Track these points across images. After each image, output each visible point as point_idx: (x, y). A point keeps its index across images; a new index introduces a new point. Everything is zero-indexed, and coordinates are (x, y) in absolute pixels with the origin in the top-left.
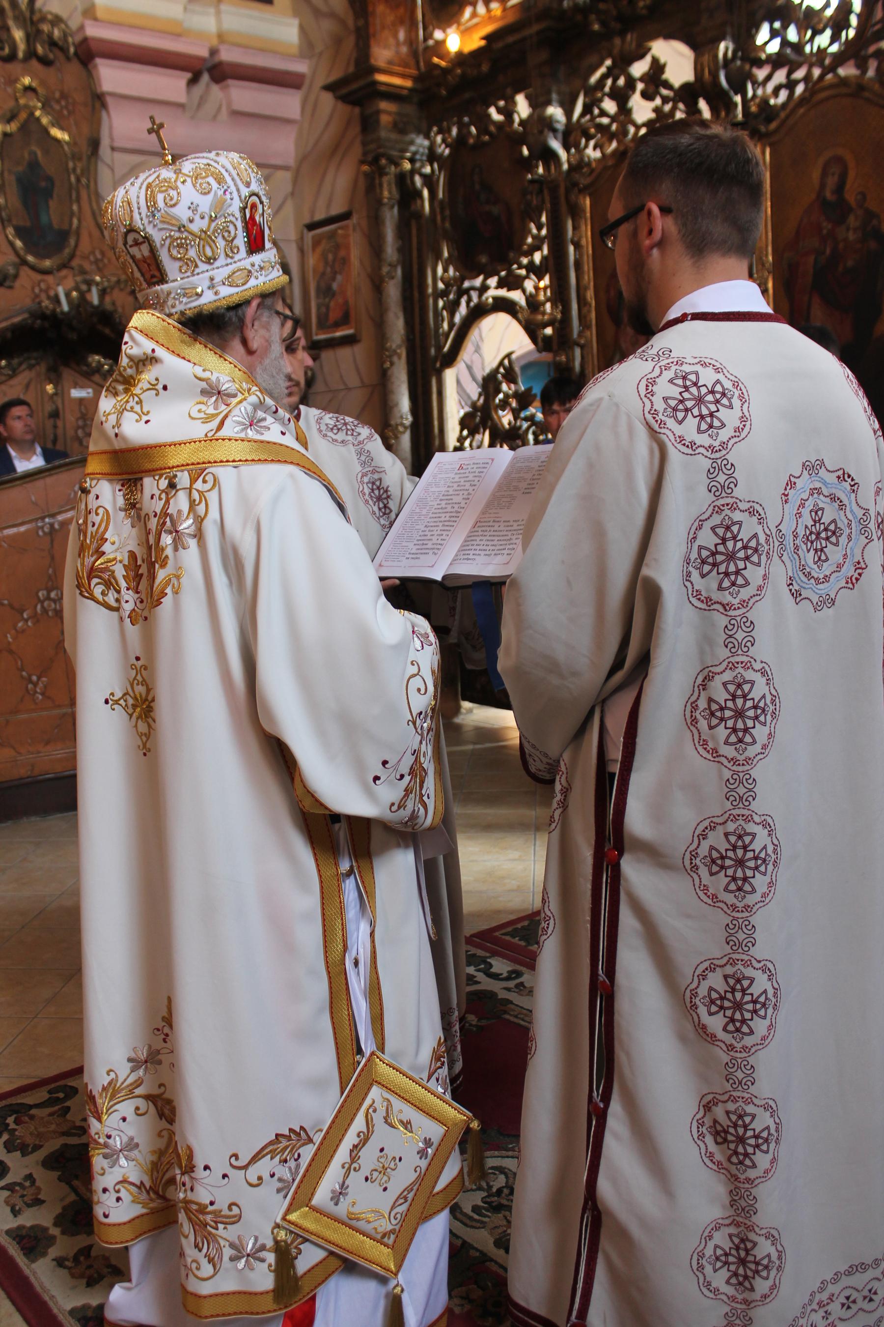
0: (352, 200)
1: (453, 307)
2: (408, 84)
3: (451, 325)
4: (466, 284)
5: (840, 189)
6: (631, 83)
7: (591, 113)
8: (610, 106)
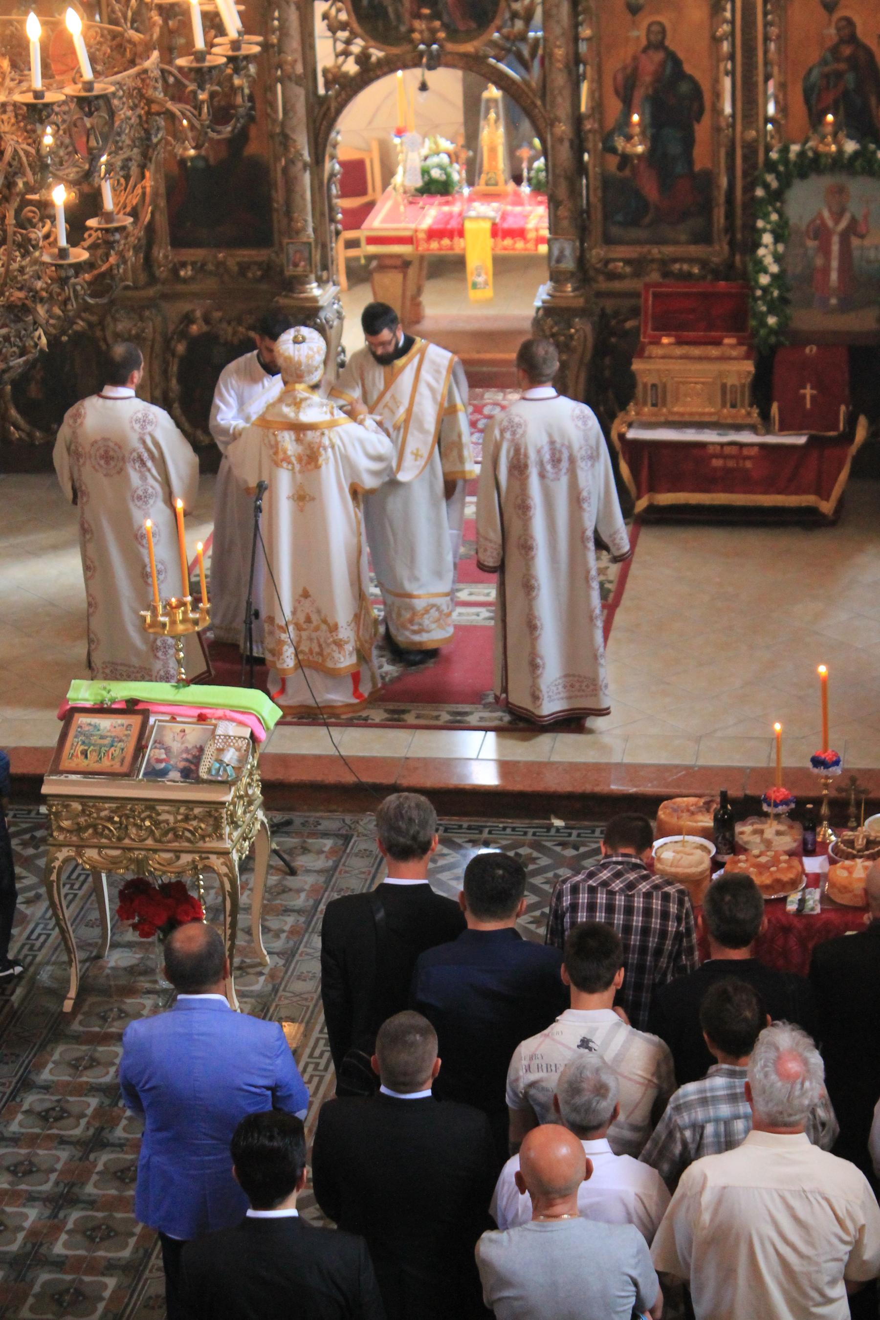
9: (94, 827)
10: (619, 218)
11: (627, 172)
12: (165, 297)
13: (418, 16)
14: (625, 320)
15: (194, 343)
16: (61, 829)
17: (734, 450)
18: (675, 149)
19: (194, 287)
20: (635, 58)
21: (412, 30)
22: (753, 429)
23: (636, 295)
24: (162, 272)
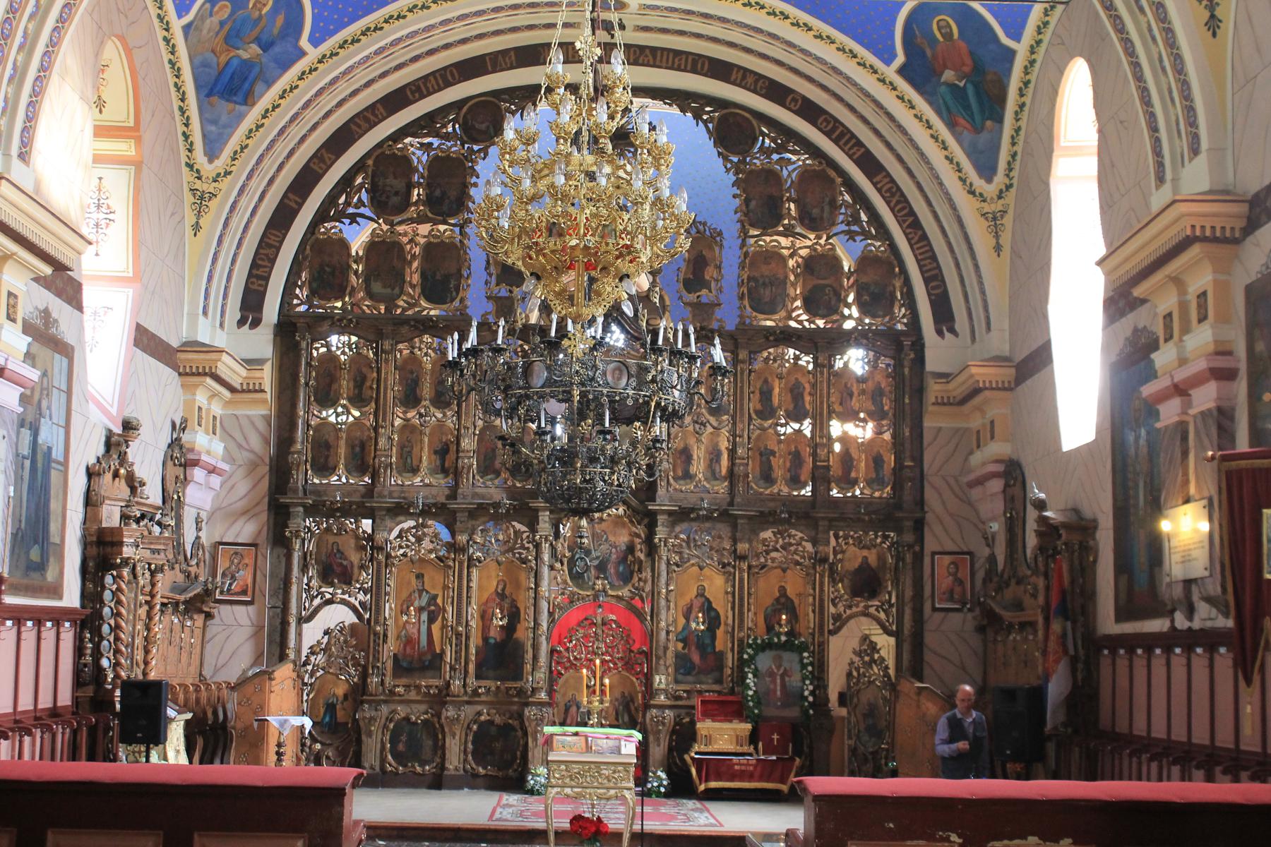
0: (255, 539)
1: (313, 598)
2: (310, 502)
3: (311, 604)
4: (323, 590)
5: (503, 590)
6: (424, 535)
7: (402, 538)
8: (413, 540)
9: (571, 776)
10: (682, 671)
11: (686, 651)
12: (468, 703)
13: (598, 578)
15: (482, 725)
16: (554, 777)
19: (483, 698)
21: (594, 584)
22: (750, 755)
24: (469, 690)
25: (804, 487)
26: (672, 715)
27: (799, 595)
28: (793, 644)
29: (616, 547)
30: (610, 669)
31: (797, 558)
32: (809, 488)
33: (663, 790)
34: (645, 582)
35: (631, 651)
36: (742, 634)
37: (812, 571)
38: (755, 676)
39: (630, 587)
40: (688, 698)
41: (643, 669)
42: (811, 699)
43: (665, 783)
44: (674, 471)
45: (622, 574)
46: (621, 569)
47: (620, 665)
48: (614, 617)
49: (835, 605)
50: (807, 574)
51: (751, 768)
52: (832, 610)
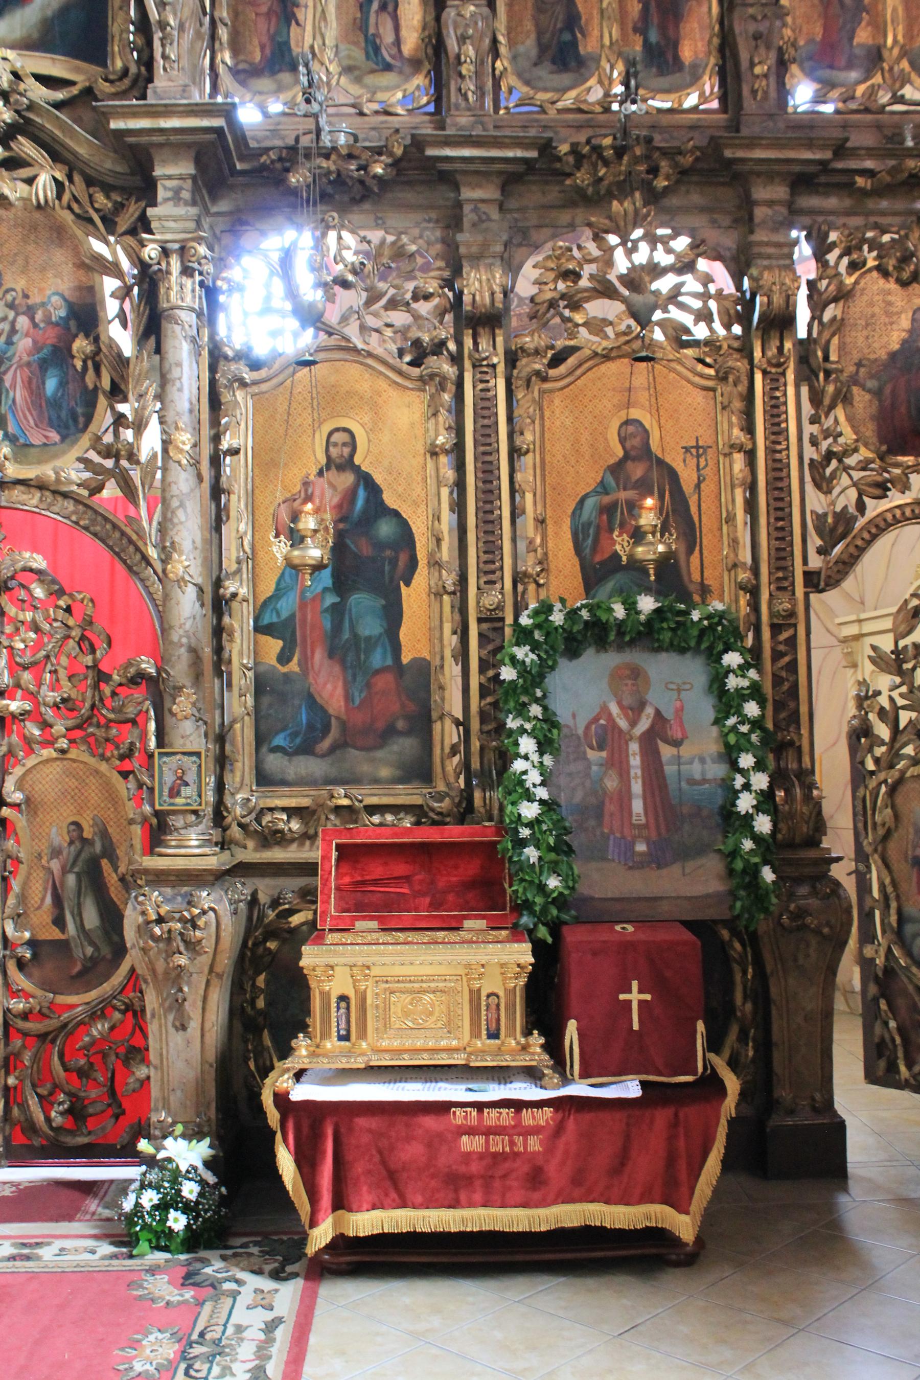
10: (279, 740)
11: (293, 666)
14: (292, 912)
17: (506, 1116)
18: (371, 627)
20: (306, 484)
22: (532, 1074)
23: (309, 869)
25: (695, 79)
26: (224, 909)
27: (697, 450)
28: (682, 626)
29: (30, 312)
30: (29, 744)
31: (687, 319)
32: (710, 84)
33: (177, 1221)
34: (139, 426)
35: (101, 677)
36: (491, 599)
37: (742, 365)
38: (542, 748)
39: (82, 446)
40: (307, 837)
41: (144, 736)
42: (763, 824)
43: (190, 1190)
44: (236, 48)
45: (55, 404)
46: (51, 385)
47: (59, 728)
48: (39, 562)
49: (824, 484)
50: (722, 378)
51: (534, 1144)
52: (816, 501)
